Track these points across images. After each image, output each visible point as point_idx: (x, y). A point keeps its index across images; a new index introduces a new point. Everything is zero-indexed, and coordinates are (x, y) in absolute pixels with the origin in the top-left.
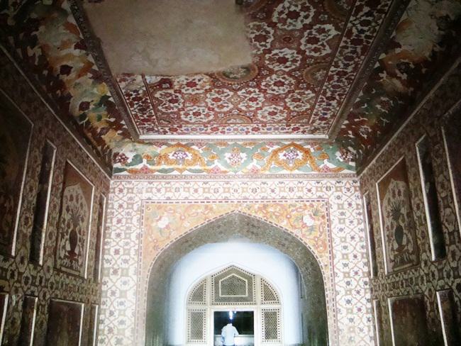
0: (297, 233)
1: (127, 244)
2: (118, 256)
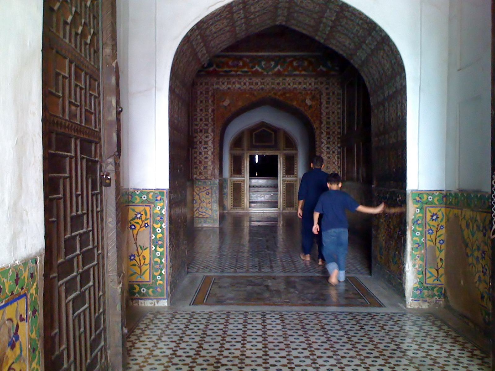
0: (302, 109)
1: (207, 115)
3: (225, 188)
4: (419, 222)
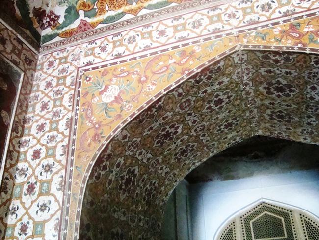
1: (52, 138)
2: (38, 161)
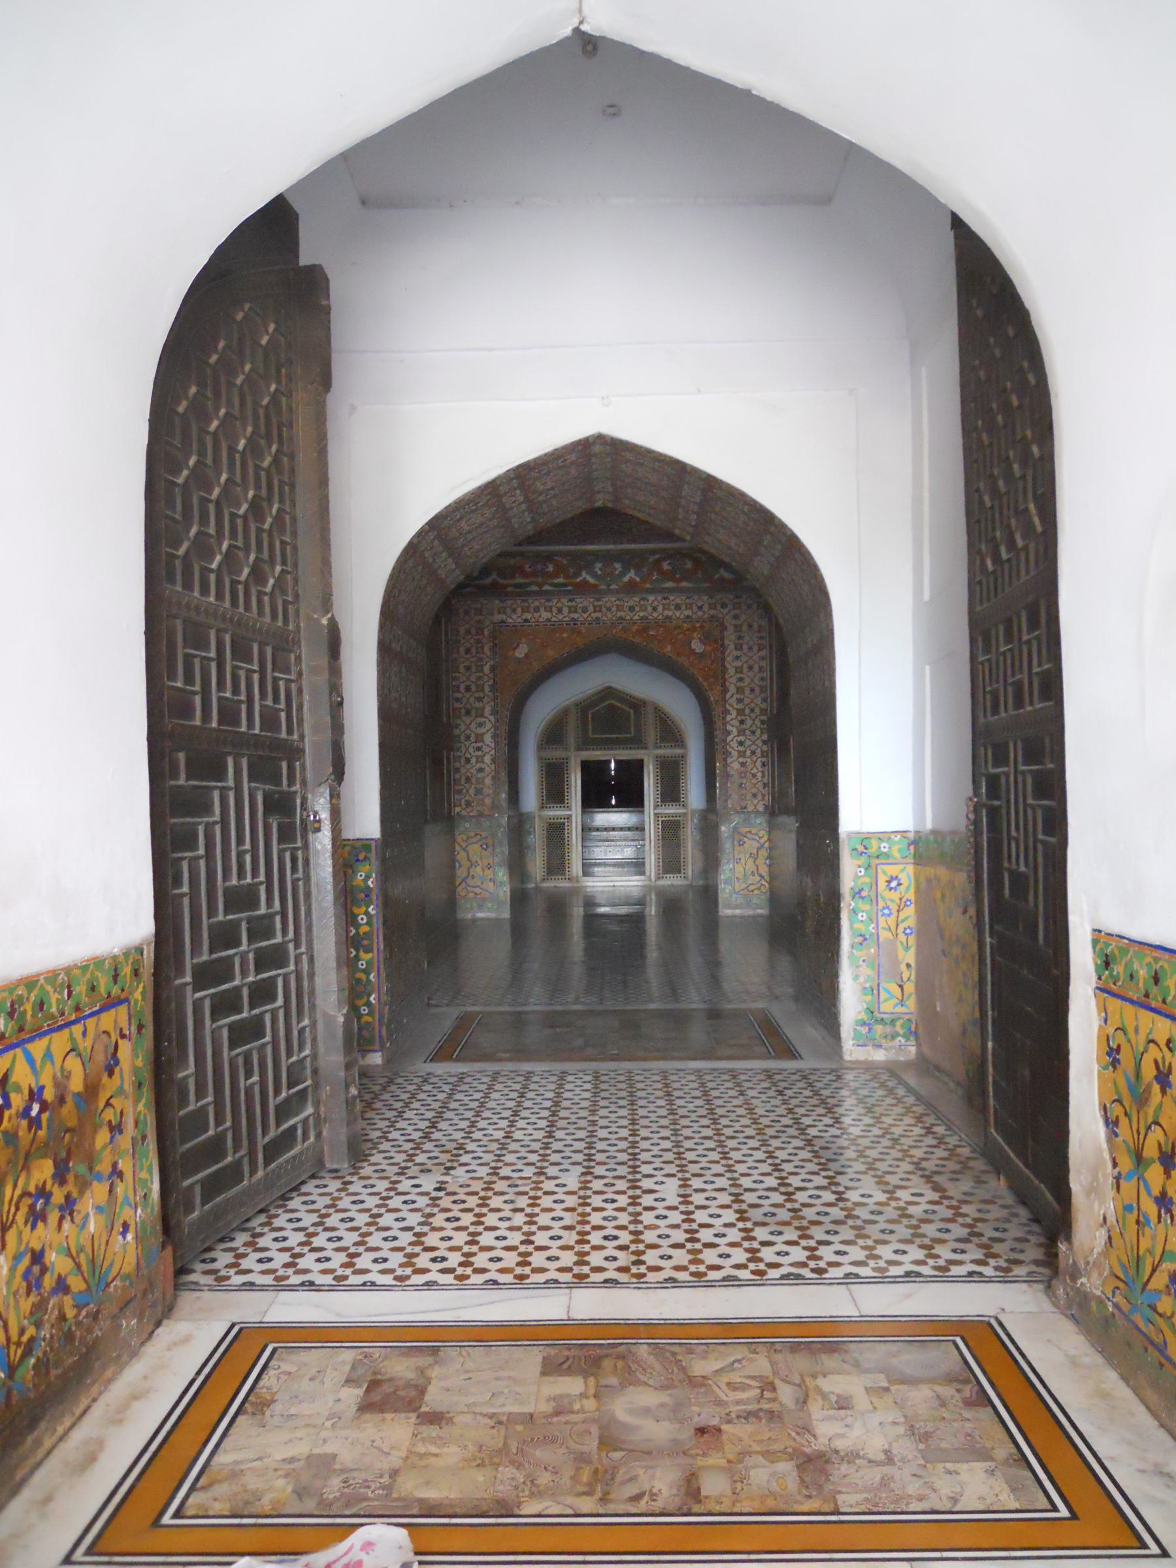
0: (683, 660)
1: (479, 678)
3: (530, 833)
4: (864, 894)
